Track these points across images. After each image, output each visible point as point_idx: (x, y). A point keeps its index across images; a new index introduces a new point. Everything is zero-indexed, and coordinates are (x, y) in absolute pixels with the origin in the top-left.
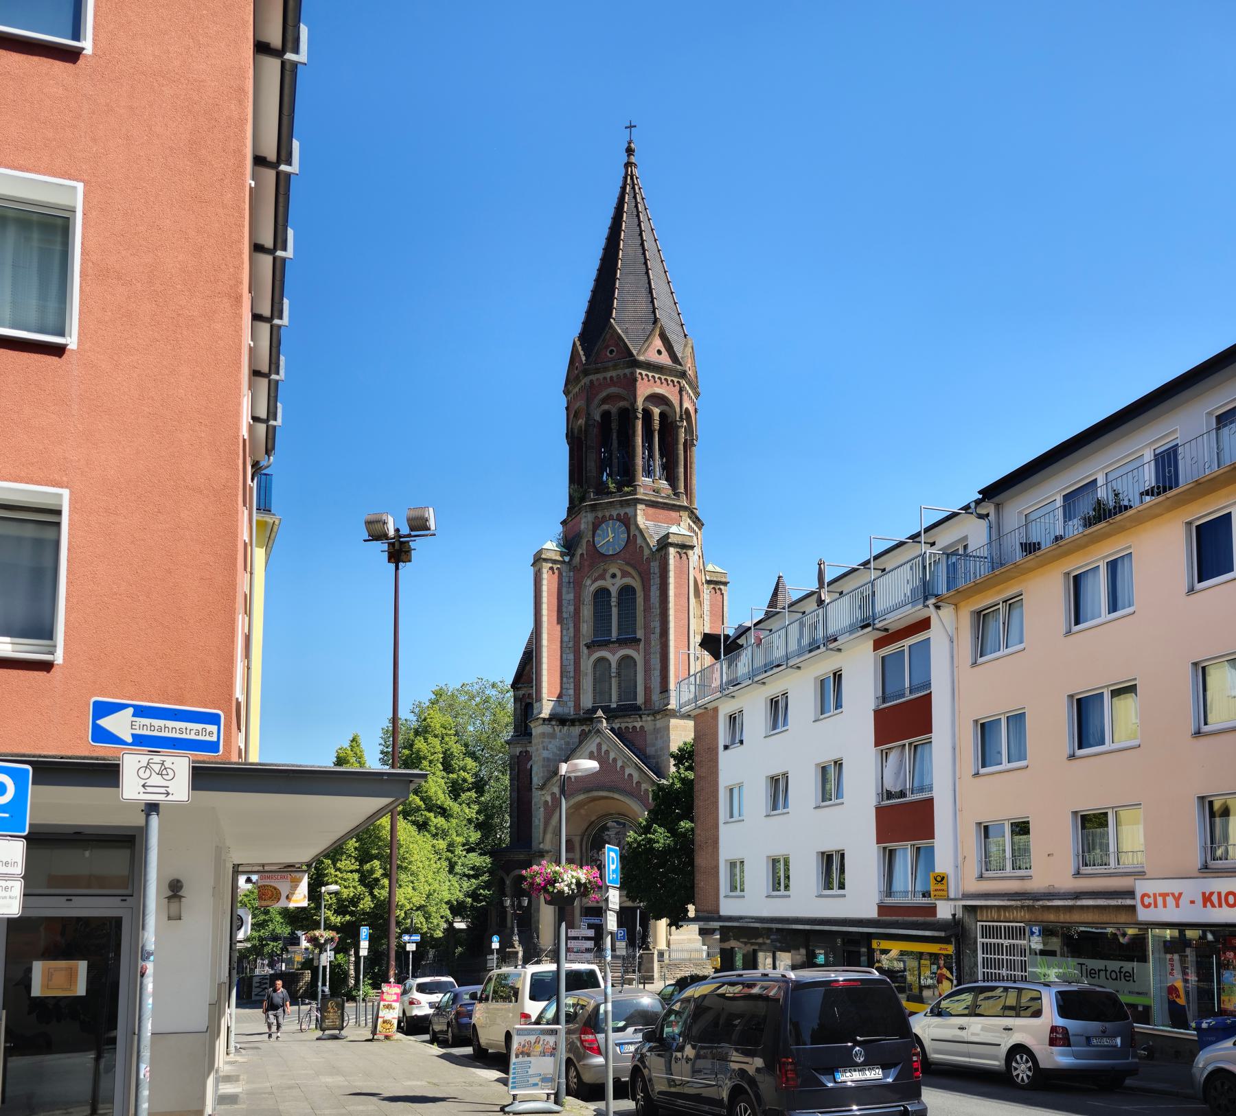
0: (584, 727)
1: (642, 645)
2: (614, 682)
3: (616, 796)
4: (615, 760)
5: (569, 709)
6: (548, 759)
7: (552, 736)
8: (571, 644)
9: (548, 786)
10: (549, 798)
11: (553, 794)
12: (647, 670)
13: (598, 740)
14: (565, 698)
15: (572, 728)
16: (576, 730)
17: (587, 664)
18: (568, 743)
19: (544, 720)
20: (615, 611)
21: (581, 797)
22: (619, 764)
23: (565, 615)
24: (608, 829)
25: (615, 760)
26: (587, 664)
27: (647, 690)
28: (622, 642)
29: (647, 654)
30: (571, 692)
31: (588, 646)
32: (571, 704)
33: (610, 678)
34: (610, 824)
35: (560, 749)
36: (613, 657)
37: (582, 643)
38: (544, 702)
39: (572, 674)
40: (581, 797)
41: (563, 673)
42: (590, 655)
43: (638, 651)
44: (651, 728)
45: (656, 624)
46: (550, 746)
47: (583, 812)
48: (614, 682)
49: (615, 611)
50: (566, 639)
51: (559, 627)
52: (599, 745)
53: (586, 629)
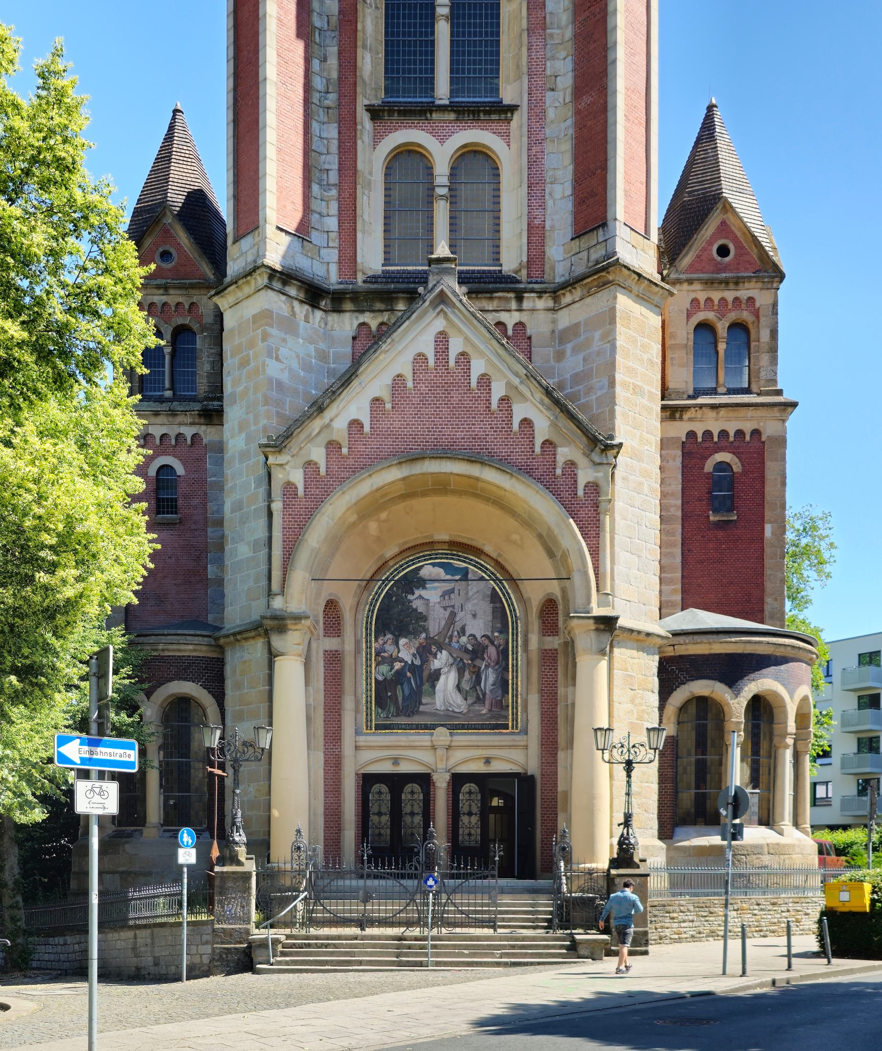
0: (366, 318)
1: (519, 121)
2: (441, 212)
3: (489, 475)
4: (485, 381)
5: (327, 270)
6: (280, 384)
7: (289, 325)
8: (332, 99)
9: (294, 444)
10: (297, 477)
11: (310, 466)
12: (535, 185)
13: (439, 324)
14: (316, 237)
15: (333, 318)
16: (346, 324)
17: (373, 159)
18: (323, 356)
19: (273, 273)
20: (443, 31)
21: (393, 475)
22: (498, 391)
23: (317, 22)
24: (422, 583)
25: (485, 381)
26: (373, 159)
27: (536, 233)
28: (463, 113)
29: (535, 141)
30: (332, 223)
31: (375, 113)
32: (333, 255)
33: (430, 198)
34: (428, 571)
35: (306, 367)
36: (442, 147)
37: (362, 102)
38: (270, 230)
39: (334, 177)
40: (393, 475)
41: (310, 172)
42: (377, 139)
43: (506, 136)
44: (546, 329)
45: (562, 68)
46: (283, 352)
47: (373, 527)
48: (441, 212)
49: (443, 31)
50: (318, 83)
51: (299, 47)
52: (442, 340)
53: (370, 64)
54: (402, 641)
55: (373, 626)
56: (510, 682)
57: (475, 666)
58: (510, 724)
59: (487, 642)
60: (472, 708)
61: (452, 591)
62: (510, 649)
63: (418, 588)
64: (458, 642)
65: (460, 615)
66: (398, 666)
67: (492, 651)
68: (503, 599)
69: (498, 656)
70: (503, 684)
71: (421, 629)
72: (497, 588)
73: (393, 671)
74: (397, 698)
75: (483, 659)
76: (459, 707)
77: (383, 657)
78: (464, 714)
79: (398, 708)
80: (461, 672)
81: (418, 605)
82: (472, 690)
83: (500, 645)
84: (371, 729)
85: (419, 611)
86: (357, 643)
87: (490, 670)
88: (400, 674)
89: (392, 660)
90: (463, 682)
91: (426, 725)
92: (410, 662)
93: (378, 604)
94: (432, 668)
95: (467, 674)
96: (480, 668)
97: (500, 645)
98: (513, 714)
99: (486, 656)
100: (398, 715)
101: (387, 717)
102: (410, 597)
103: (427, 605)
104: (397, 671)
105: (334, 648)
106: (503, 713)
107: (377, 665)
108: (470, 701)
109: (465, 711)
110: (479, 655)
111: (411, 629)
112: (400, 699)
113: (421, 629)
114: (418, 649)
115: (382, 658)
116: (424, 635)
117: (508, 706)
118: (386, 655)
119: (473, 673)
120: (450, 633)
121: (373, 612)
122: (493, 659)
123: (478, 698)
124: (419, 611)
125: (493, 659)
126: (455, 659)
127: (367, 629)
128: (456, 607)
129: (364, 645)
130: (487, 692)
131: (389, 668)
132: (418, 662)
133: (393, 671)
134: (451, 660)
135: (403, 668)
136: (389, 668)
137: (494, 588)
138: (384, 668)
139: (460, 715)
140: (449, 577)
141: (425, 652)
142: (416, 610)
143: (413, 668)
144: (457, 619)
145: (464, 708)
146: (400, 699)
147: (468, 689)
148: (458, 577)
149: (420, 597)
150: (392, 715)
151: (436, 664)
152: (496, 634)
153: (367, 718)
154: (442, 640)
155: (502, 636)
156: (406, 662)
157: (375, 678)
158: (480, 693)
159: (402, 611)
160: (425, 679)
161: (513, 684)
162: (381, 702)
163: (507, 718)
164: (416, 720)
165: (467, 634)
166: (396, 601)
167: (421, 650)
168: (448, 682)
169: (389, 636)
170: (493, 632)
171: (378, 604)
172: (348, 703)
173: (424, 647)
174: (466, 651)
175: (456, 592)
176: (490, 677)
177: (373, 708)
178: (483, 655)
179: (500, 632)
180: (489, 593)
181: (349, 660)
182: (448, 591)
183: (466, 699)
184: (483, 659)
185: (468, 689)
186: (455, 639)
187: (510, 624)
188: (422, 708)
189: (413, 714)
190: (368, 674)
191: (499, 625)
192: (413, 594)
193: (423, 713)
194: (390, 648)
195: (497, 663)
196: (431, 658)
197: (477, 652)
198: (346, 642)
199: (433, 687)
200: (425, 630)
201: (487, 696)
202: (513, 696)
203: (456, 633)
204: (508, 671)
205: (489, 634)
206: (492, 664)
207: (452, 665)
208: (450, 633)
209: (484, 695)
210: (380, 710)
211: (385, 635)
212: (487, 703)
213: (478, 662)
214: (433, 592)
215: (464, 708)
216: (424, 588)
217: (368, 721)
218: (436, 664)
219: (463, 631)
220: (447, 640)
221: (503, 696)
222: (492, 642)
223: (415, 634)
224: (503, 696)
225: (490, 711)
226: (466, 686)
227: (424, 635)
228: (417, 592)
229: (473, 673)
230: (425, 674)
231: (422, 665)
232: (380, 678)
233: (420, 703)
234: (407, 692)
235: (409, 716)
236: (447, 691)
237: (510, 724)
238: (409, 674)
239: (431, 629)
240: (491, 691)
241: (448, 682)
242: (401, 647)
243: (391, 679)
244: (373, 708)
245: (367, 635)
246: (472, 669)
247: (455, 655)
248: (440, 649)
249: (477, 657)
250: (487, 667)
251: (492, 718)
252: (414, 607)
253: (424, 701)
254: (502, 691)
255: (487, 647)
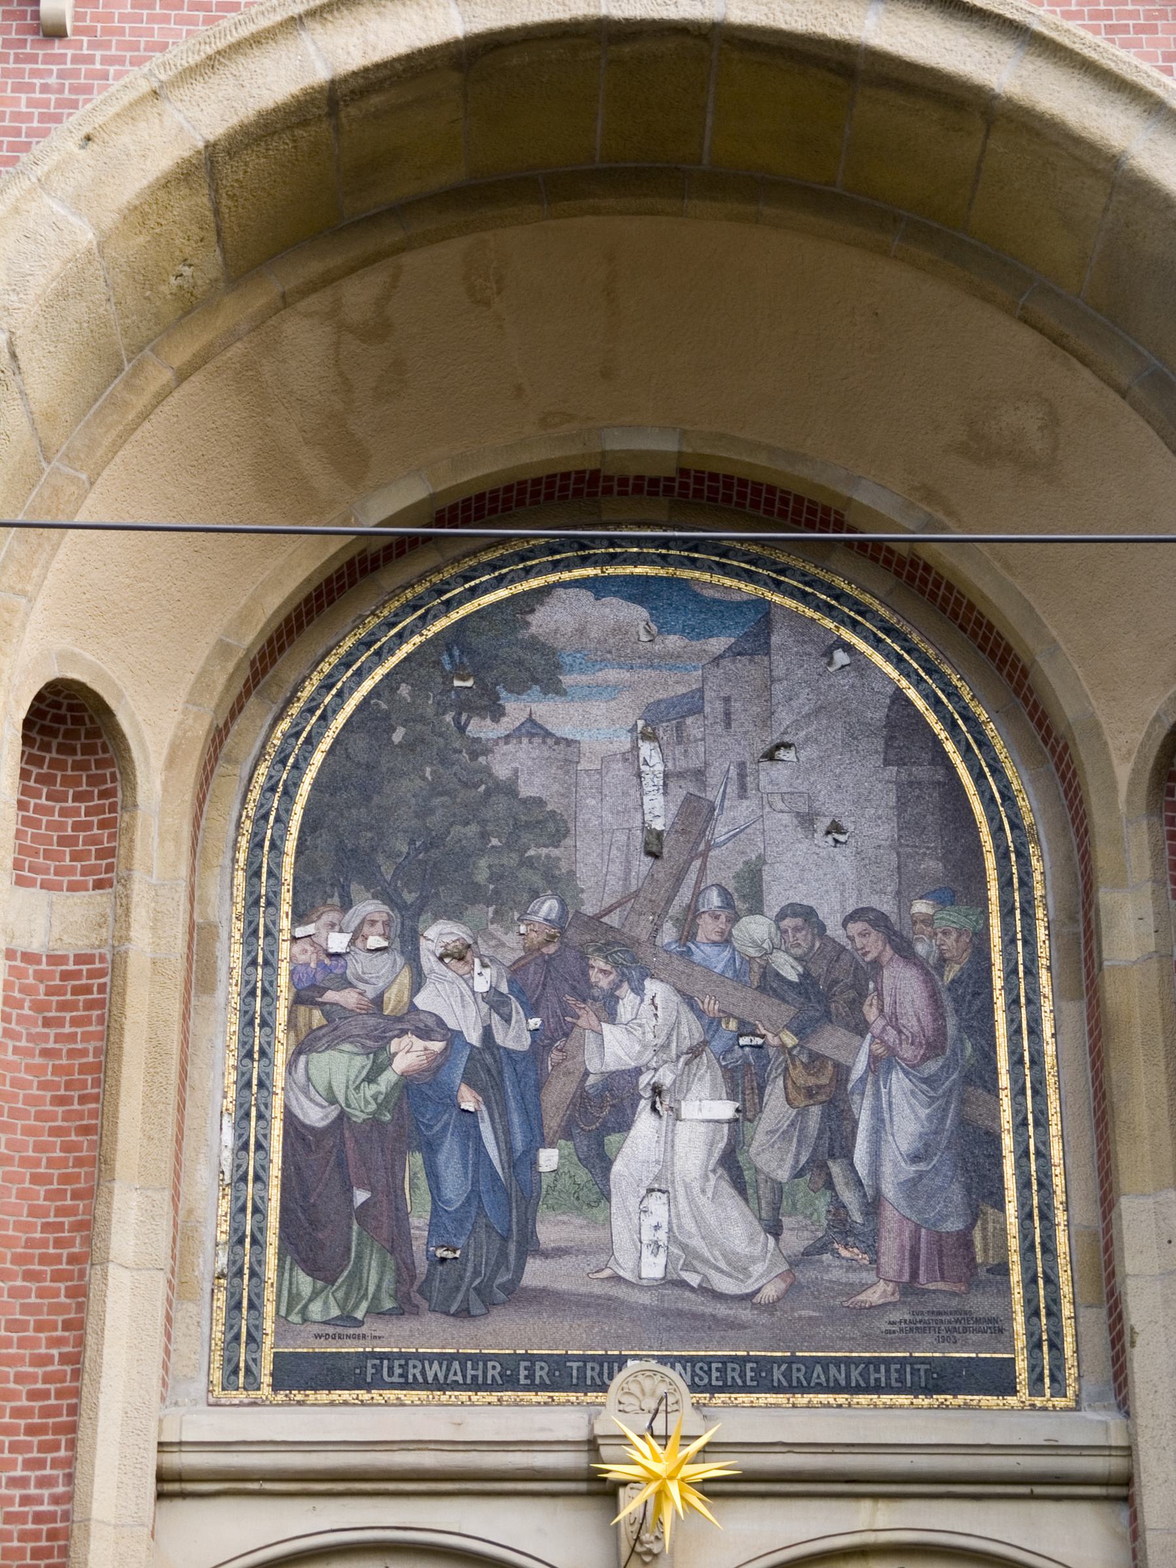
24: (543, 671)
54: (439, 934)
55: (288, 861)
56: (1008, 1142)
57: (816, 1061)
58: (1021, 1365)
59: (873, 945)
60: (808, 1274)
61: (693, 705)
62: (998, 983)
63: (518, 688)
64: (726, 941)
65: (734, 814)
66: (409, 1054)
67: (904, 990)
68: (949, 747)
69: (938, 1013)
70: (971, 1154)
71: (537, 880)
72: (912, 693)
73: (387, 1079)
74: (400, 1217)
75: (861, 1028)
76: (739, 1268)
77: (331, 1012)
78: (770, 1307)
79: (404, 1272)
80: (745, 1081)
81: (516, 764)
82: (802, 1174)
83: (943, 961)
84: (253, 1382)
85: (525, 791)
86: (200, 937)
87: (899, 1082)
88: (420, 1095)
89: (380, 1026)
90: (760, 1138)
91: (558, 1363)
92: (474, 1037)
93: (318, 758)
94: (593, 1066)
95: (775, 1094)
96: (842, 1072)
97: (943, 961)
98: (1032, 1313)
99: (871, 1013)
100: (404, 1308)
101: (346, 1319)
102: (481, 728)
103: (568, 764)
104: (408, 1084)
105: (75, 941)
106: (981, 1304)
107: (301, 1049)
108: (795, 1240)
109: (771, 1292)
110: (838, 1006)
111: (482, 877)
112: (419, 1220)
113: (537, 880)
114: (516, 972)
115: (323, 1011)
116: (548, 907)
117: (1003, 1269)
118: (347, 998)
119: (810, 1093)
120: (685, 895)
121: (289, 795)
122: (910, 1023)
123: (840, 1226)
124: (525, 791)
125: (910, 1023)
126: (712, 1025)
127: (254, 874)
128: (714, 777)
129: (238, 951)
130: (889, 1190)
131: (362, 1063)
132: (515, 1035)
133: (387, 1079)
134: (690, 1030)
135: (437, 1067)
136: (362, 1063)
137: (899, 696)
138: (338, 1066)
139: (745, 1314)
140: (674, 642)
141: (556, 984)
142: (509, 789)
143: (488, 1064)
144: (721, 831)
145: (764, 1276)
146: (419, 1220)
147: (783, 1175)
148: (718, 644)
149: (533, 729)
150: (376, 1311)
151: (615, 1046)
152: (921, 907)
153: (229, 1326)
154: (642, 931)
155: (952, 918)
156: (454, 1038)
157: (290, 1118)
158: (849, 1197)
159: (437, 789)
160: (553, 1122)
161: (1022, 1155)
162: (311, 1241)
163: (999, 1328)
164: (502, 1334)
165: (775, 900)
166: (409, 746)
167: (533, 976)
168: (673, 1148)
169: (369, 907)
170: (902, 897)
171: (318, 758)
172: (132, 1224)
173: (549, 961)
174: (769, 983)
175: (712, 708)
176: (897, 1123)
177: (271, 1274)
178: (856, 1005)
179: (944, 897)
180: (877, 715)
181: (146, 1007)
182: (672, 703)
183: (774, 1229)
184: (861, 1028)
185: (783, 1175)
186: (708, 928)
187: (990, 862)
188: (535, 1273)
189: (490, 1304)
190: (252, 1089)
191: (933, 866)
192: (497, 713)
193: (542, 1297)
194: (377, 973)
195: (934, 1046)
196: (587, 1018)
197: (828, 991)
198: (140, 916)
199: (600, 1163)
200: (556, 880)
201: (890, 1217)
202: (1026, 1217)
203: (714, 899)
204: (993, 1089)
205: (886, 905)
206: (907, 1052)
207: (695, 1052)
208: (685, 895)
209: (873, 1205)
210: (305, 1283)
211: (346, 905)
212: (891, 1247)
213: (831, 1042)
214: (598, 708)
215: (764, 1276)
216: (552, 687)
217: (239, 1339)
218: (615, 1046)
219: (749, 892)
220: (668, 934)
221: (975, 1215)
222: (904, 950)
223: (506, 897)
224: (975, 1215)
225: (909, 1289)
226: (772, 1159)
227: (548, 907)
228: (516, 709)
229: (810, 1093)
230: (556, 1097)
231: (542, 1042)
232: (315, 1115)
233: (529, 1246)
234: (455, 1187)
235: (465, 1313)
236: (669, 1196)
237: (1021, 1365)
238: (468, 1100)
239: (585, 877)
240: (911, 1187)
241: (673, 1148)
242: (428, 961)
243: (374, 1121)
244: (271, 1274)
245: (253, 903)
246: (800, 1076)
247: (711, 1006)
248: (634, 969)
249: (827, 1016)
250: (880, 1065)
251: (915, 1329)
252: (502, 771)
253: (548, 1232)
254: (968, 1190)
255: (877, 965)
